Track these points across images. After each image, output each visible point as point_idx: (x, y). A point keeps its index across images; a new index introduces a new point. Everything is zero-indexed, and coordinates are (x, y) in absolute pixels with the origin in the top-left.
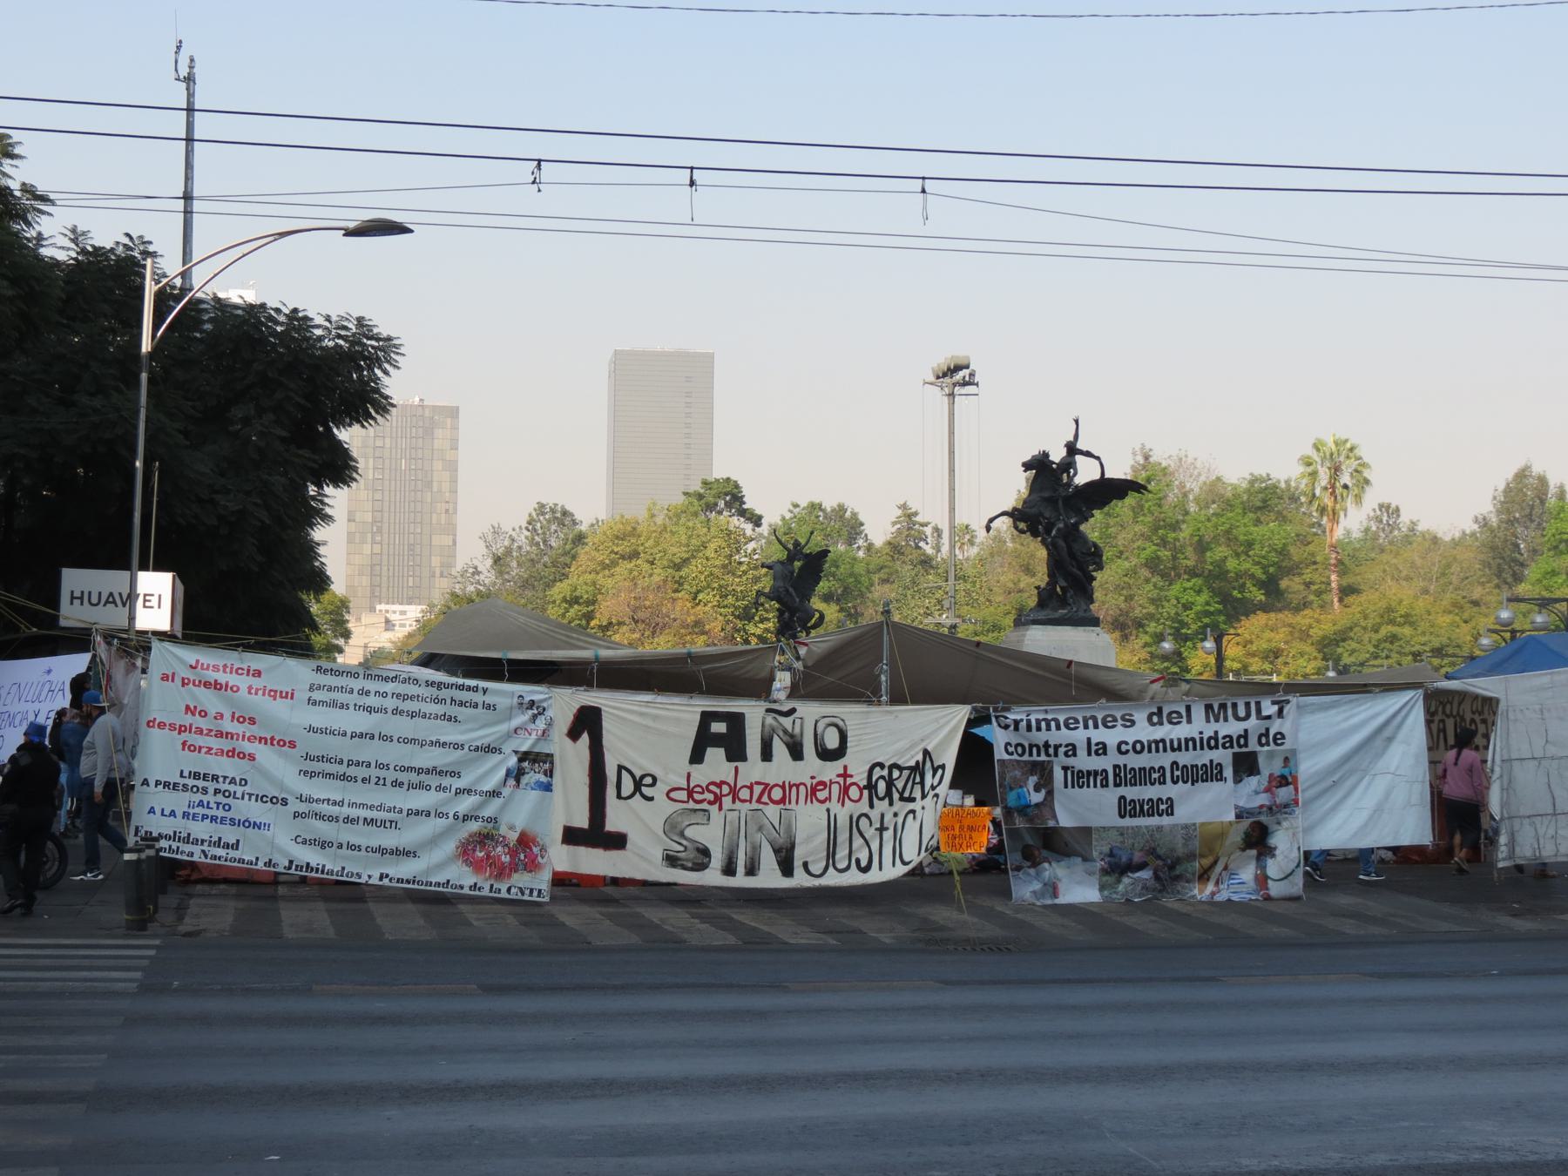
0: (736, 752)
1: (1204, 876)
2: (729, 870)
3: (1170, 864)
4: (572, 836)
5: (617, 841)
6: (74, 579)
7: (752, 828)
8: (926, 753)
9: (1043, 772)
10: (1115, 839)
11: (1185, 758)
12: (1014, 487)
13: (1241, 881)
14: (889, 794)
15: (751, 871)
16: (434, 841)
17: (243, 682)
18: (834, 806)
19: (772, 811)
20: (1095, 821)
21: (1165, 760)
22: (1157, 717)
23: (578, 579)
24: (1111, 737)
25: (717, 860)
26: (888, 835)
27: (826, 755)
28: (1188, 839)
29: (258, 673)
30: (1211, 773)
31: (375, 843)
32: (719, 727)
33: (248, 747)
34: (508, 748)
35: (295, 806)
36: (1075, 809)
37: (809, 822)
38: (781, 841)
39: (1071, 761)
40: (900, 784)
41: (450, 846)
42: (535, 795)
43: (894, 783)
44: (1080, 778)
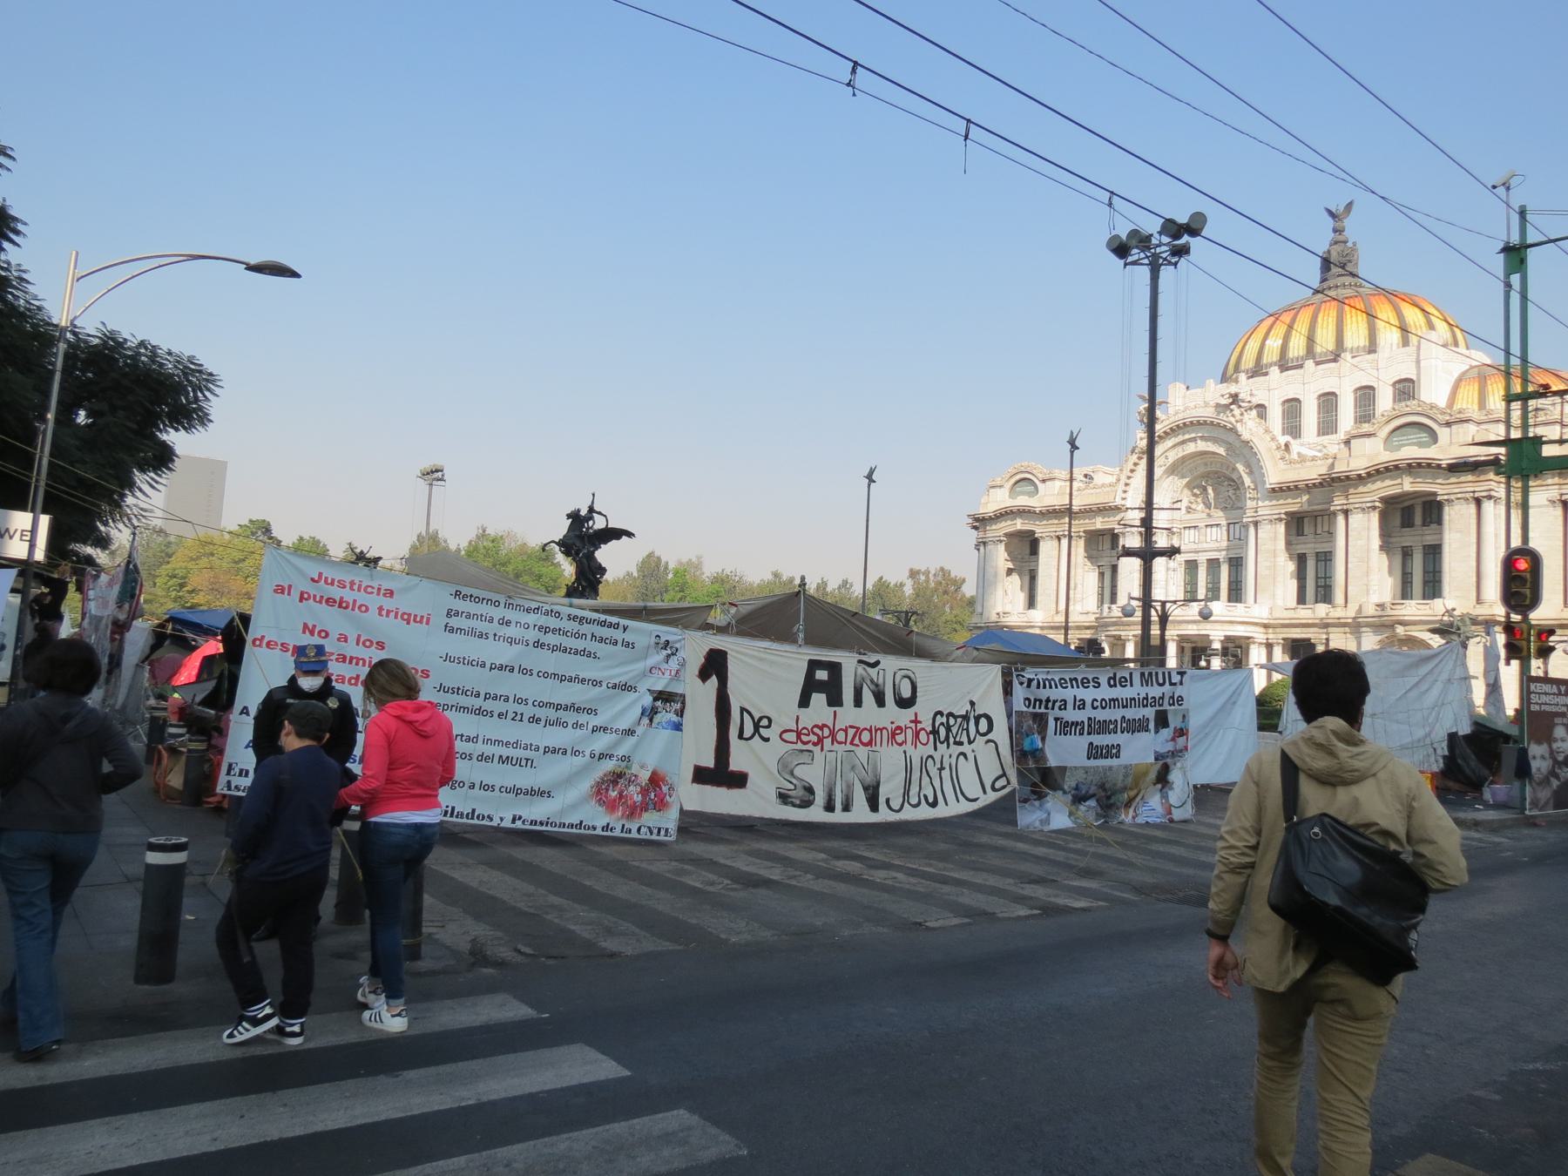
0: (835, 700)
1: (1128, 805)
2: (830, 807)
3: (1107, 797)
7: (847, 767)
8: (972, 704)
9: (1041, 720)
10: (1081, 776)
11: (1131, 713)
12: (561, 528)
13: (1151, 808)
14: (947, 738)
15: (847, 808)
16: (569, 780)
17: (374, 601)
18: (909, 747)
19: (862, 752)
23: (177, 564)
24: (1088, 694)
26: (946, 773)
27: (904, 703)
28: (1126, 776)
29: (391, 593)
30: (1137, 726)
31: (510, 785)
32: (822, 675)
34: (643, 687)
36: (1064, 751)
37: (890, 763)
38: (869, 780)
40: (954, 730)
41: (586, 785)
42: (667, 733)
43: (952, 728)
44: (1066, 727)
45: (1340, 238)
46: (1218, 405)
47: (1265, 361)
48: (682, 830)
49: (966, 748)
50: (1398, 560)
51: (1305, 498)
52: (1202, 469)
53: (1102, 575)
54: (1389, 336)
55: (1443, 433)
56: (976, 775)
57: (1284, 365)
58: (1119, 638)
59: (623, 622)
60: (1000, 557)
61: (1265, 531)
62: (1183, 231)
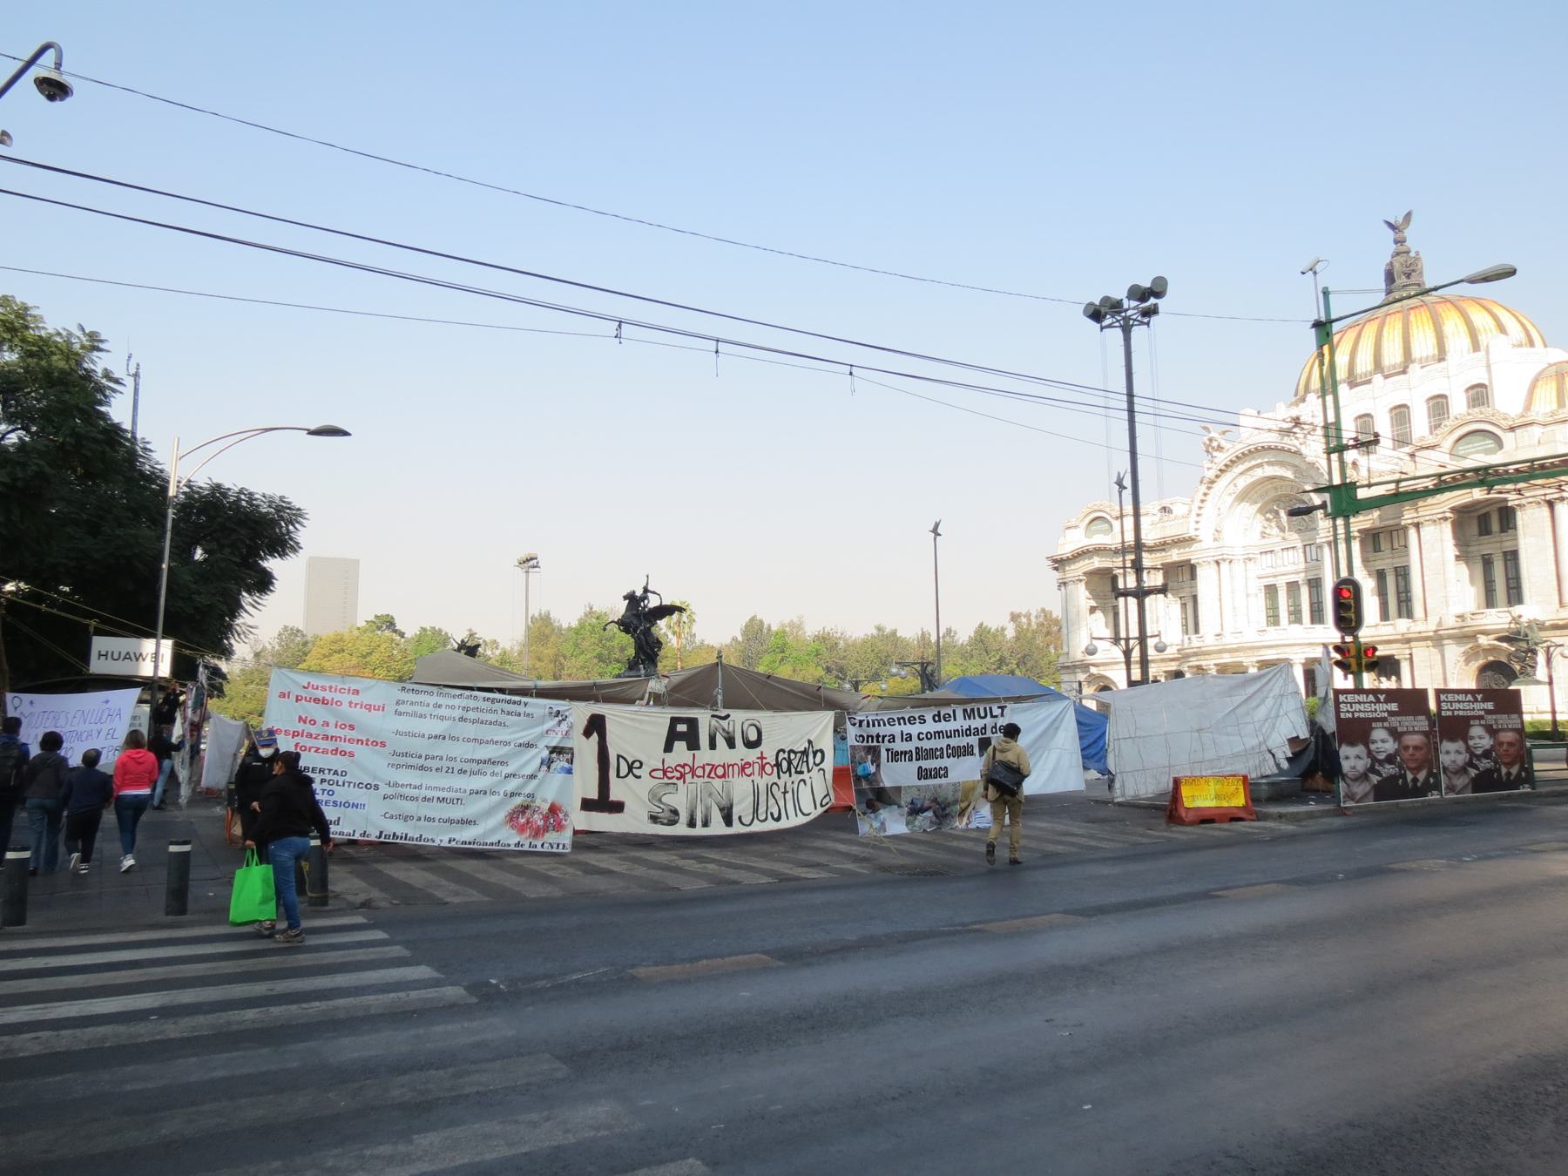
0: (693, 745)
1: (962, 813)
2: (692, 824)
4: (587, 805)
5: (618, 807)
6: (100, 644)
7: (705, 795)
8: (810, 742)
9: (874, 752)
10: (915, 793)
11: (954, 742)
12: (621, 608)
14: (789, 769)
15: (706, 824)
16: (489, 813)
17: (346, 698)
19: (717, 783)
20: (903, 783)
21: (942, 743)
22: (937, 718)
25: (684, 817)
26: (789, 796)
27: (750, 745)
28: (955, 791)
29: (357, 692)
30: (966, 751)
31: (445, 816)
32: (682, 728)
33: (347, 747)
34: (541, 745)
35: (384, 790)
36: (894, 775)
37: (741, 790)
38: (724, 803)
39: (891, 746)
40: (795, 763)
41: (501, 815)
42: (562, 776)
43: (793, 762)
44: (896, 756)
45: (1403, 249)
46: (1281, 431)
48: (576, 846)
49: (806, 776)
52: (1272, 494)
53: (1184, 605)
55: (1507, 438)
56: (810, 796)
58: (1199, 668)
59: (524, 699)
60: (1082, 596)
62: (1149, 295)
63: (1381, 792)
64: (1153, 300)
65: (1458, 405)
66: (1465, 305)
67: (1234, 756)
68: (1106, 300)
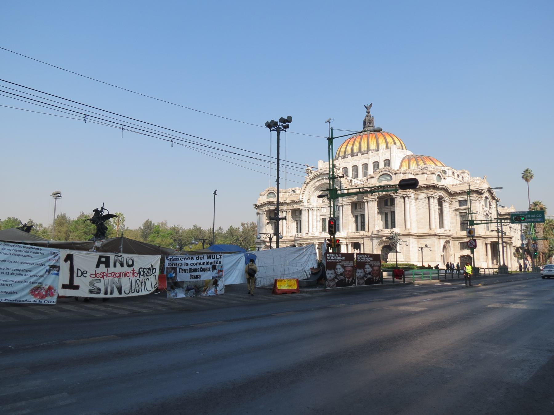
1: (205, 291)
2: (106, 293)
3: (197, 289)
4: (64, 287)
5: (77, 287)
8: (152, 265)
9: (175, 270)
11: (203, 267)
14: (144, 274)
15: (111, 293)
16: (23, 289)
18: (131, 278)
19: (116, 279)
20: (185, 280)
21: (199, 267)
22: (198, 258)
24: (189, 262)
25: (103, 291)
26: (143, 284)
27: (129, 266)
28: (203, 283)
31: (4, 290)
32: (103, 259)
34: (47, 264)
36: (182, 277)
39: (181, 267)
41: (28, 290)
44: (183, 271)
47: (347, 153)
48: (58, 302)
49: (149, 277)
50: (384, 216)
51: (356, 197)
53: (297, 223)
54: (383, 146)
55: (393, 176)
56: (150, 285)
57: (352, 155)
58: (300, 244)
59: (40, 248)
60: (265, 219)
61: (345, 208)
62: (286, 121)
63: (338, 285)
64: (287, 123)
65: (381, 165)
66: (385, 134)
67: (294, 273)
68: (272, 121)
